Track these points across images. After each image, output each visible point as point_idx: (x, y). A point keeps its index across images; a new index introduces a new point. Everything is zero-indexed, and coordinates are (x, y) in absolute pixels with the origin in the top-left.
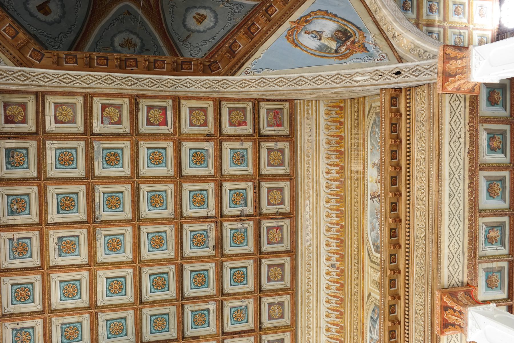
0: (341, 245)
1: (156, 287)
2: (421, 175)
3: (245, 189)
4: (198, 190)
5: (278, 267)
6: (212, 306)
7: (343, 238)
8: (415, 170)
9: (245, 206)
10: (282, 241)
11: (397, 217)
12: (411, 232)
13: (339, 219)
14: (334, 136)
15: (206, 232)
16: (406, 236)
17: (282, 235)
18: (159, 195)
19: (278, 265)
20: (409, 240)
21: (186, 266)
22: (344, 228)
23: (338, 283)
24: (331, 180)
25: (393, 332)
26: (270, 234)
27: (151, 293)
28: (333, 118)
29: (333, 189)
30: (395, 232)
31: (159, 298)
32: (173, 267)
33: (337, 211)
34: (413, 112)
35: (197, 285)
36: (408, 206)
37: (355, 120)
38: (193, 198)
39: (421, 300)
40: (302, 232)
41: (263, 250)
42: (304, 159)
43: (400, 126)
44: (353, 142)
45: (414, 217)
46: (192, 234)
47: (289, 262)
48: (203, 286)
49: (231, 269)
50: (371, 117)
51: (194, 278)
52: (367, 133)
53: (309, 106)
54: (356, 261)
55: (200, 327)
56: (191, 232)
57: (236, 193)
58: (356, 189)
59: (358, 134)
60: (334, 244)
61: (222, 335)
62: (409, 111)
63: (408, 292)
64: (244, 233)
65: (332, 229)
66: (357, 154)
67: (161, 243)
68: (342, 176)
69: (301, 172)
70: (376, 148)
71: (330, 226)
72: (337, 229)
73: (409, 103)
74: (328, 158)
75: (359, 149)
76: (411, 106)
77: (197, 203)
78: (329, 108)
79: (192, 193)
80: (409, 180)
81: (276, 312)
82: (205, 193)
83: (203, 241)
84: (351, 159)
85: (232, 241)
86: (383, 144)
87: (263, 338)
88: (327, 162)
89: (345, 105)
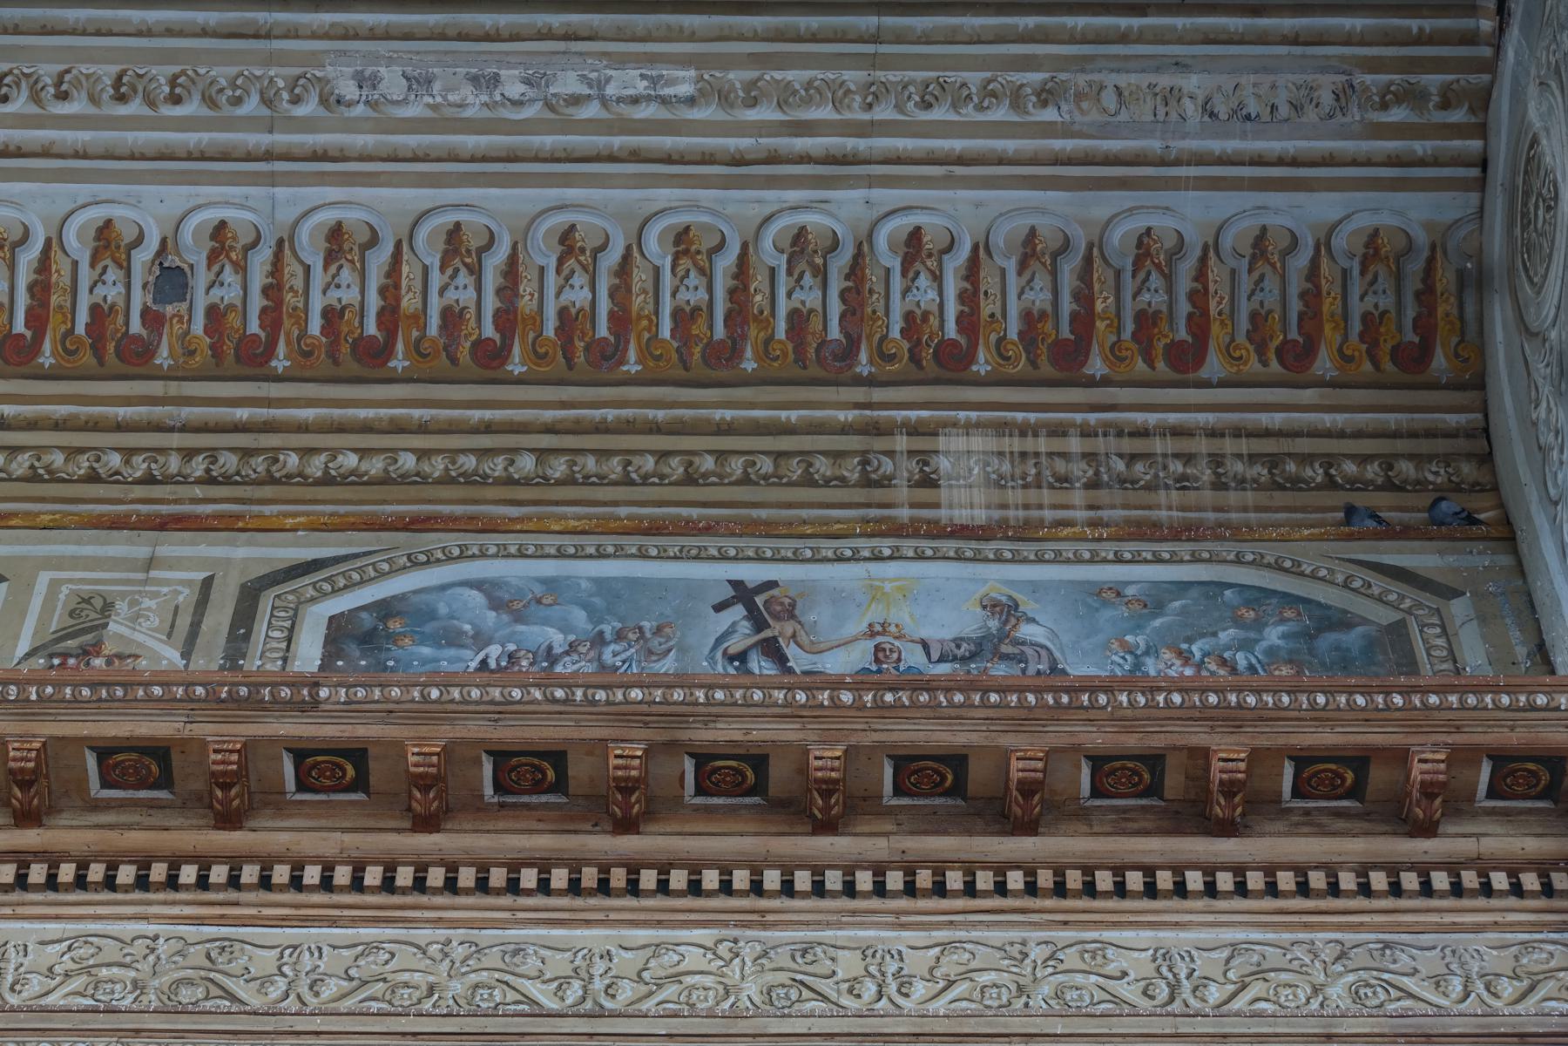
0: (345, 349)
2: (985, 978)
7: (399, 363)
8: (1015, 935)
11: (649, 800)
12: (539, 900)
13: (550, 330)
14: (1199, 297)
16: (514, 867)
20: (482, 885)
23: (37, 319)
24: (855, 271)
28: (1337, 290)
29: (782, 292)
30: (538, 787)
33: (612, 316)
36: (741, 879)
37: (1329, 461)
39: (35, 979)
40: (443, 37)
42: (1027, 63)
43: (1340, 824)
44: (1158, 445)
45: (660, 924)
50: (1365, 592)
52: (1238, 561)
53: (1445, 105)
54: (229, 462)
58: (795, 469)
59: (1219, 485)
60: (350, 296)
62: (1457, 890)
63: (81, 882)
65: (464, 278)
66: (1064, 481)
68: (891, 358)
69: (926, 39)
70: (1137, 628)
71: (495, 261)
72: (471, 314)
73: (1517, 890)
74: (1030, 250)
75: (1103, 495)
76: (1494, 903)
78: (1415, 267)
80: (940, 889)
84: (1024, 431)
86: (1213, 699)
88: (998, 240)
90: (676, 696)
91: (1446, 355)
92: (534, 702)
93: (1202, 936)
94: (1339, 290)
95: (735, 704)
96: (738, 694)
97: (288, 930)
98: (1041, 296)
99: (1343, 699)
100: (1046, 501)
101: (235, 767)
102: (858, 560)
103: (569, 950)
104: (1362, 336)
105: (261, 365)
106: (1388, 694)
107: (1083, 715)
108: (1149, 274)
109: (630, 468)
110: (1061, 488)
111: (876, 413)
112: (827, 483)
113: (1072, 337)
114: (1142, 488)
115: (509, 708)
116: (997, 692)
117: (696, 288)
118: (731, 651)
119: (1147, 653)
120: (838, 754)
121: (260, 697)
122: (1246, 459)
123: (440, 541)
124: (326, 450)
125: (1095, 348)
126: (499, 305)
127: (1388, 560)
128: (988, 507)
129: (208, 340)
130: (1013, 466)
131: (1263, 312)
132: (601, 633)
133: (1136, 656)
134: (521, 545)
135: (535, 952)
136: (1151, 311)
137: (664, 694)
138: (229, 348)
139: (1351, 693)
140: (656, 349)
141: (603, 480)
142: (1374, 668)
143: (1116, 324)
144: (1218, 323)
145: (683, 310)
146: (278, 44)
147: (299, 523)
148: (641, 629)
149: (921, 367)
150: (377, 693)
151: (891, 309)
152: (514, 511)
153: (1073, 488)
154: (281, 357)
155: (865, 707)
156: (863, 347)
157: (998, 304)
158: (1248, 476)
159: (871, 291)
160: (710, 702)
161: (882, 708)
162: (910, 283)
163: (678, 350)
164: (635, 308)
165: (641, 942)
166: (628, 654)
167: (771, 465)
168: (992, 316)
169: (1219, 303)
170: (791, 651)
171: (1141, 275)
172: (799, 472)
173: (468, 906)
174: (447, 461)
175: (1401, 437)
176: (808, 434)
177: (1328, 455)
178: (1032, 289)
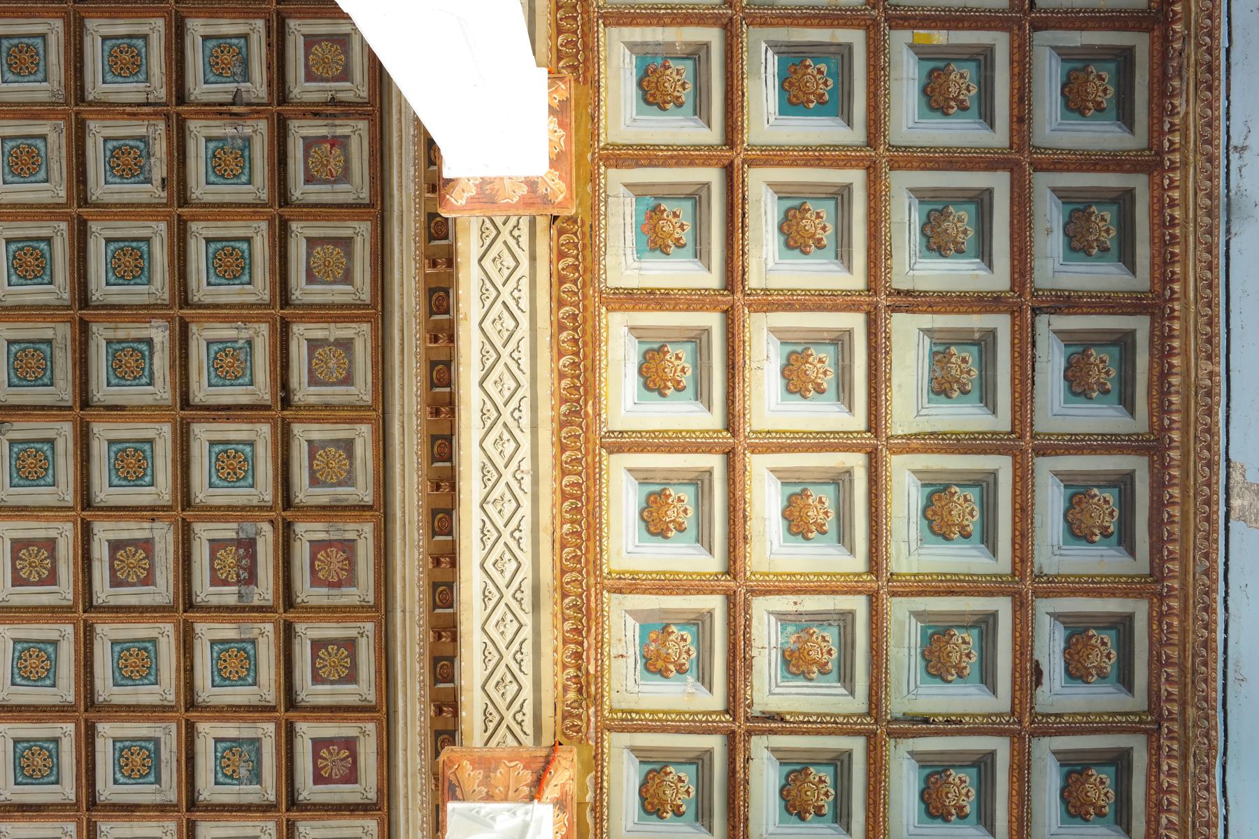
1: (21, 271)
3: (245, 37)
4: (122, 37)
5: (336, 245)
6: (159, 334)
9: (244, 82)
10: (345, 176)
15: (145, 142)
17: (347, 161)
18: (28, 46)
19: (336, 241)
21: (94, 226)
25: (442, 294)
26: (313, 157)
27: (9, 285)
31: (28, 300)
32: (63, 226)
35: (123, 277)
38: (111, 55)
41: (294, 198)
46: (110, 145)
47: (367, 236)
48: (138, 281)
49: (209, 241)
51: (114, 257)
55: (129, 383)
56: (106, 140)
57: (219, 46)
61: (182, 409)
64: (242, 150)
67: (33, 163)
77: (122, 69)
79: (109, 43)
81: (330, 365)
82: (140, 43)
83: (135, 164)
85: (210, 169)
87: (295, 432)
146: (404, 209)
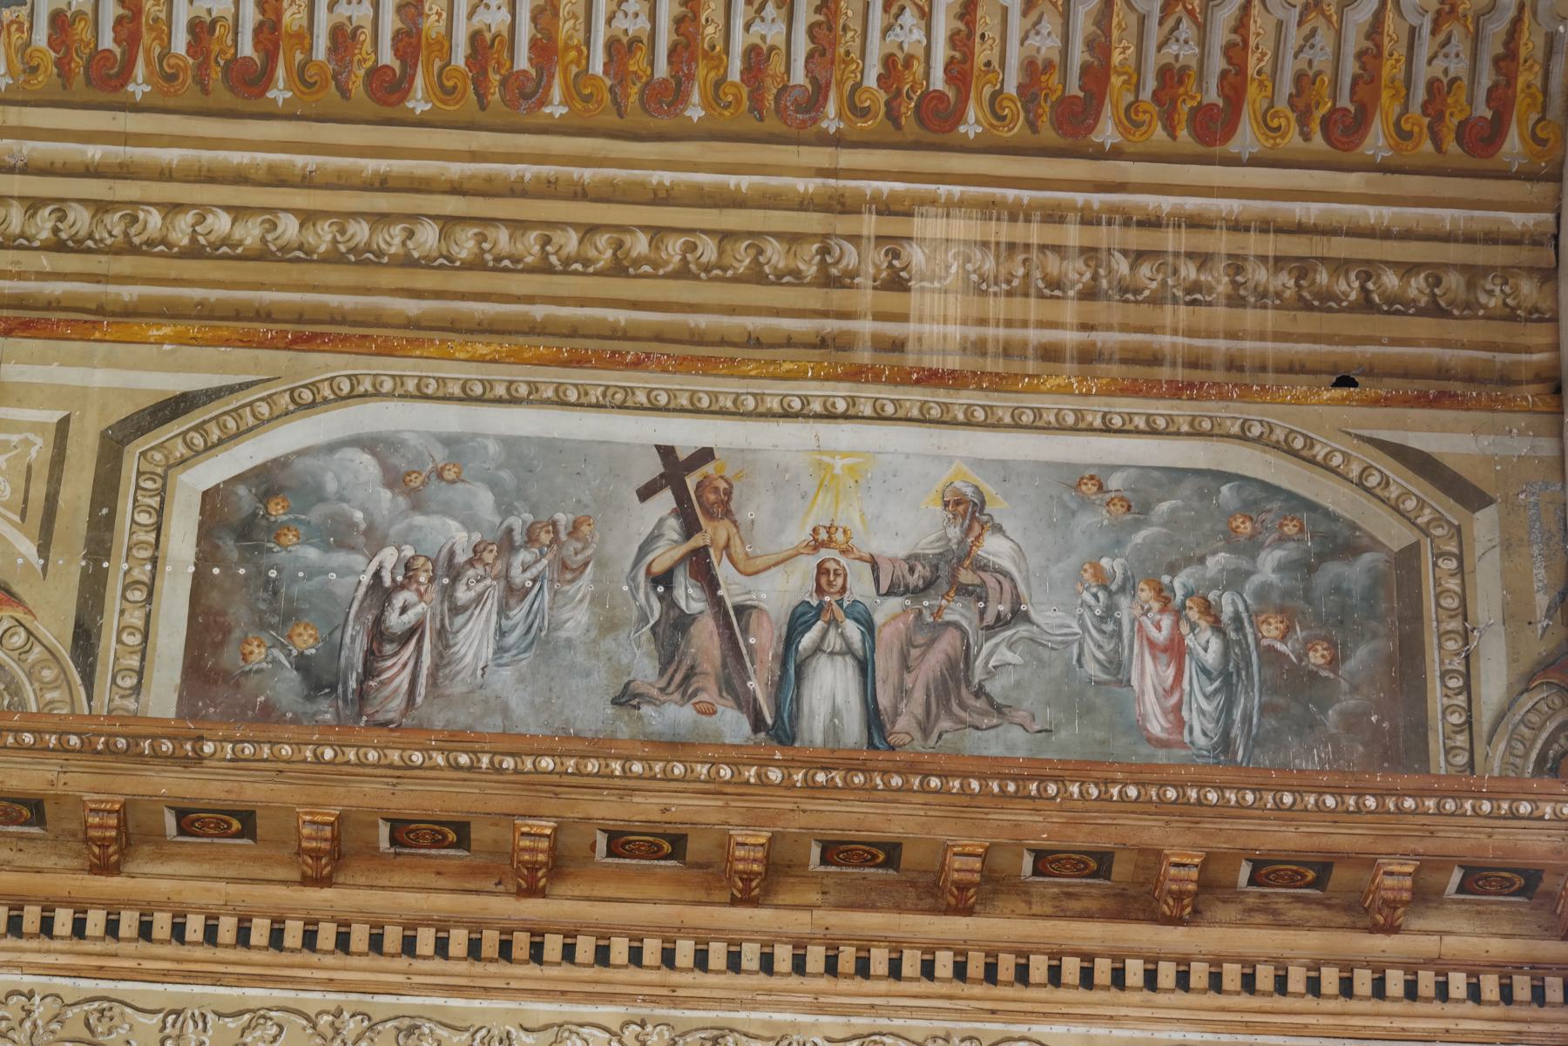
0: (216, 74)
7: (279, 93)
13: (460, 58)
14: (1236, 52)
22: (372, 108)
28: (1401, 51)
29: (738, 23)
33: (534, 44)
34: (1399, 1023)
37: (1368, 270)
54: (80, 218)
58: (742, 258)
59: (1235, 301)
68: (864, 113)
72: (366, 36)
75: (1099, 310)
84: (1015, 213)
86: (1171, 794)
89: (1503, 175)
90: (590, 768)
91: (1521, 136)
92: (436, 767)
93: (1137, 1034)
94: (1404, 51)
95: (654, 778)
96: (658, 767)
97: (170, 988)
98: (1049, 42)
99: (1311, 800)
100: (1032, 317)
101: (113, 833)
102: (806, 416)
103: (467, 1030)
104: (1425, 106)
105: (116, 89)
106: (1360, 795)
107: (1029, 804)
108: (1179, 21)
109: (549, 248)
110: (1052, 297)
111: (841, 183)
112: (778, 282)
113: (1081, 94)
114: (1143, 302)
115: (409, 773)
116: (939, 776)
117: (636, 15)
118: (658, 568)
119: (1122, 589)
120: (762, 841)
121: (138, 750)
122: (1271, 262)
123: (327, 367)
124: (194, 206)
125: (1107, 109)
126: (400, 25)
127: (1416, 440)
128: (964, 322)
129: (53, 54)
130: (998, 264)
131: (1311, 73)
132: (510, 531)
133: (1110, 594)
134: (421, 378)
135: (431, 1031)
136: (1177, 66)
137: (577, 765)
138: (78, 65)
139: (1321, 794)
140: (585, 87)
141: (515, 265)
142: (1374, 624)
143: (1134, 80)
144: (1256, 84)
145: (619, 41)
147: (165, 335)
148: (554, 524)
149: (898, 126)
150: (266, 751)
151: (868, 51)
152: (412, 307)
153: (1064, 298)
154: (140, 80)
155: (794, 786)
156: (832, 95)
157: (997, 50)
158: (1271, 289)
159: (845, 28)
160: (626, 774)
161: (813, 788)
162: (892, 20)
163: (611, 90)
164: (562, 36)
165: (543, 1021)
166: (540, 567)
167: (715, 250)
168: (988, 64)
169: (1260, 60)
170: (723, 570)
171: (1170, 23)
172: (747, 261)
173: (359, 968)
174: (335, 228)
175: (1456, 241)
176: (760, 207)
177: (1368, 262)
178: (1038, 33)
